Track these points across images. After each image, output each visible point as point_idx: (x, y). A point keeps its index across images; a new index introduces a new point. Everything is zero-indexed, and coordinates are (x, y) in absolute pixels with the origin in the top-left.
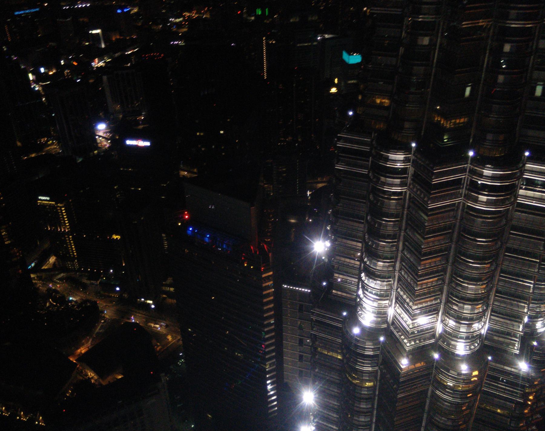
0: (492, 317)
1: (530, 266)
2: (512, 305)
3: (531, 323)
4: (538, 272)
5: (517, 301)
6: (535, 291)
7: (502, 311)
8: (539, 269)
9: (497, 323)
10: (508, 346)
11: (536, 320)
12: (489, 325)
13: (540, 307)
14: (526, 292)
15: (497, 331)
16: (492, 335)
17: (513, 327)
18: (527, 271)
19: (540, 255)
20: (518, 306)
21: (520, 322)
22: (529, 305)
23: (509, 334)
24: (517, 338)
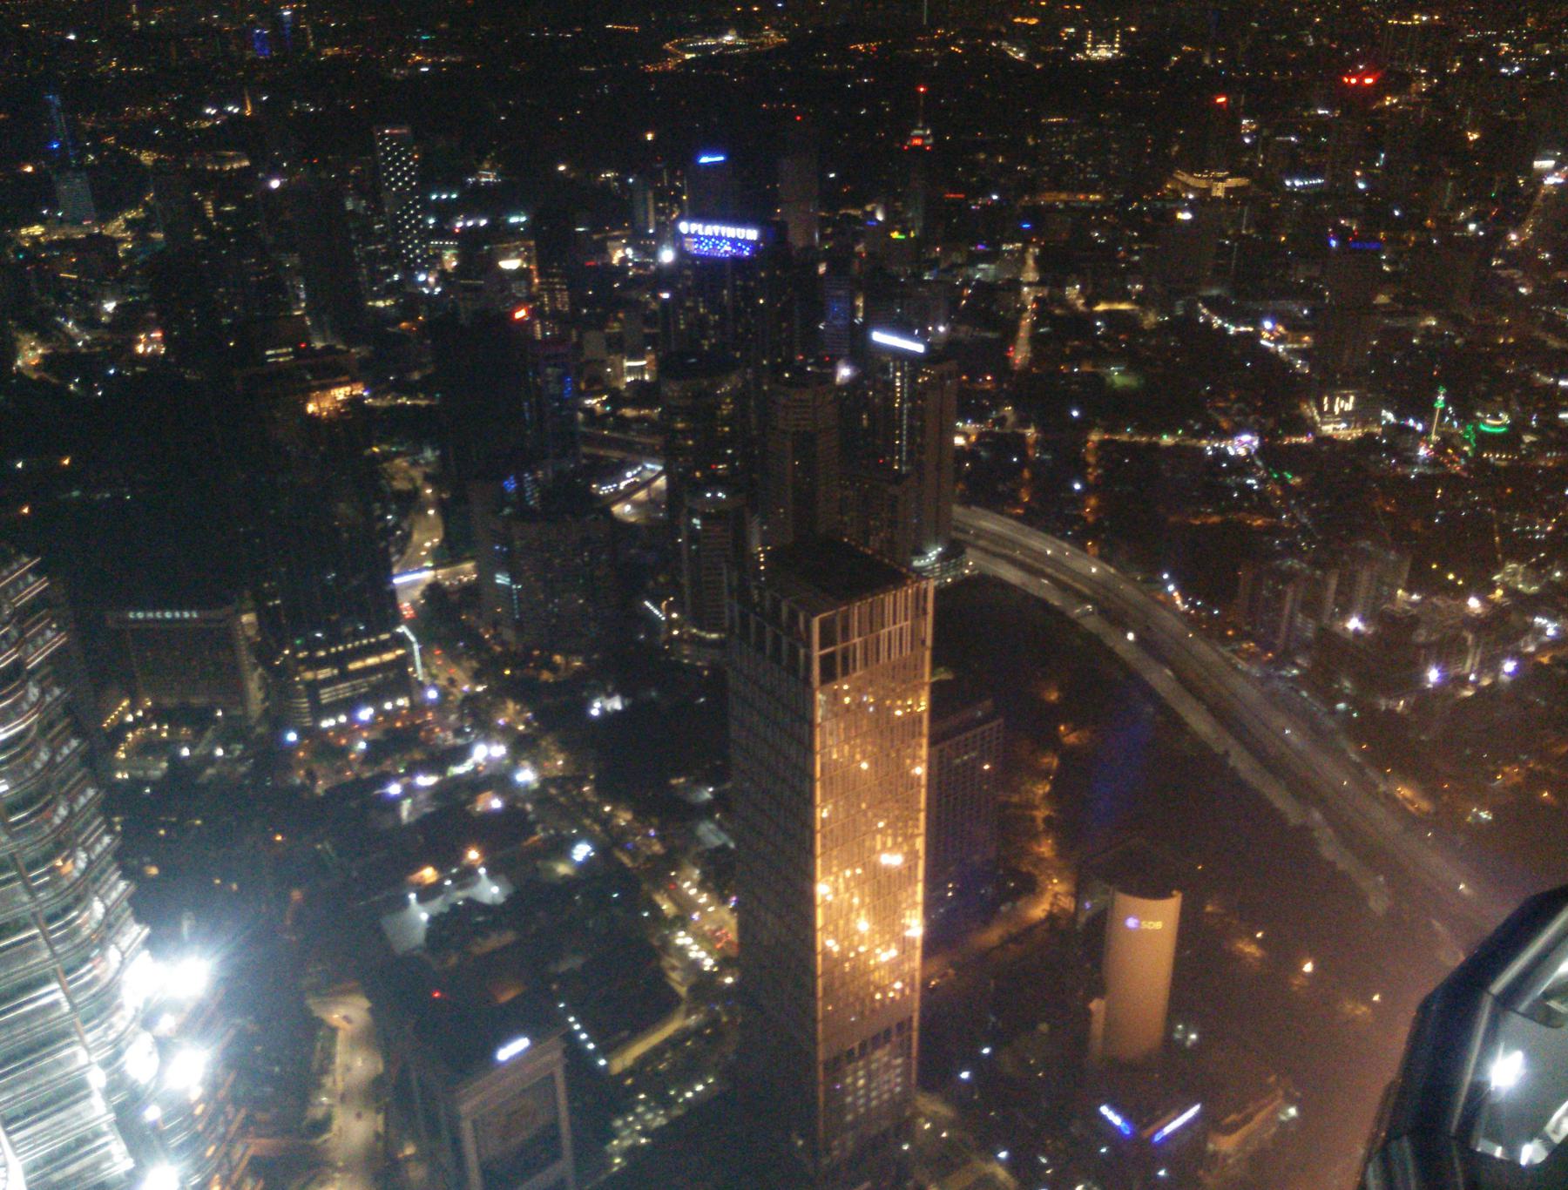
0: (16, 1137)
1: (26, 955)
2: (41, 1072)
3: (116, 1076)
4: (54, 954)
5: (49, 1054)
6: (77, 1001)
7: (31, 1101)
8: (50, 945)
9: (35, 1140)
10: (97, 1168)
11: (122, 1060)
12: (21, 1160)
13: (111, 1027)
14: (56, 1019)
15: (51, 1159)
16: (42, 1176)
17: (81, 1118)
18: (25, 972)
19: (34, 915)
20: (59, 1063)
21: (87, 1096)
22: (82, 1041)
23: (81, 1142)
24: (104, 1134)
